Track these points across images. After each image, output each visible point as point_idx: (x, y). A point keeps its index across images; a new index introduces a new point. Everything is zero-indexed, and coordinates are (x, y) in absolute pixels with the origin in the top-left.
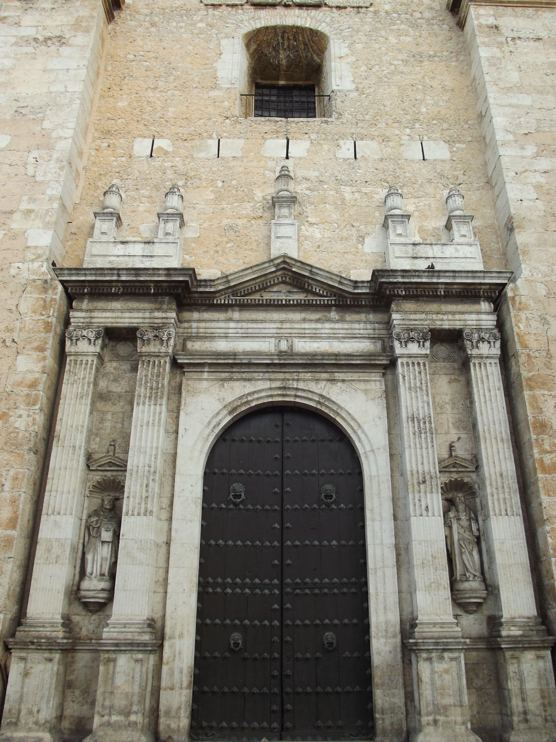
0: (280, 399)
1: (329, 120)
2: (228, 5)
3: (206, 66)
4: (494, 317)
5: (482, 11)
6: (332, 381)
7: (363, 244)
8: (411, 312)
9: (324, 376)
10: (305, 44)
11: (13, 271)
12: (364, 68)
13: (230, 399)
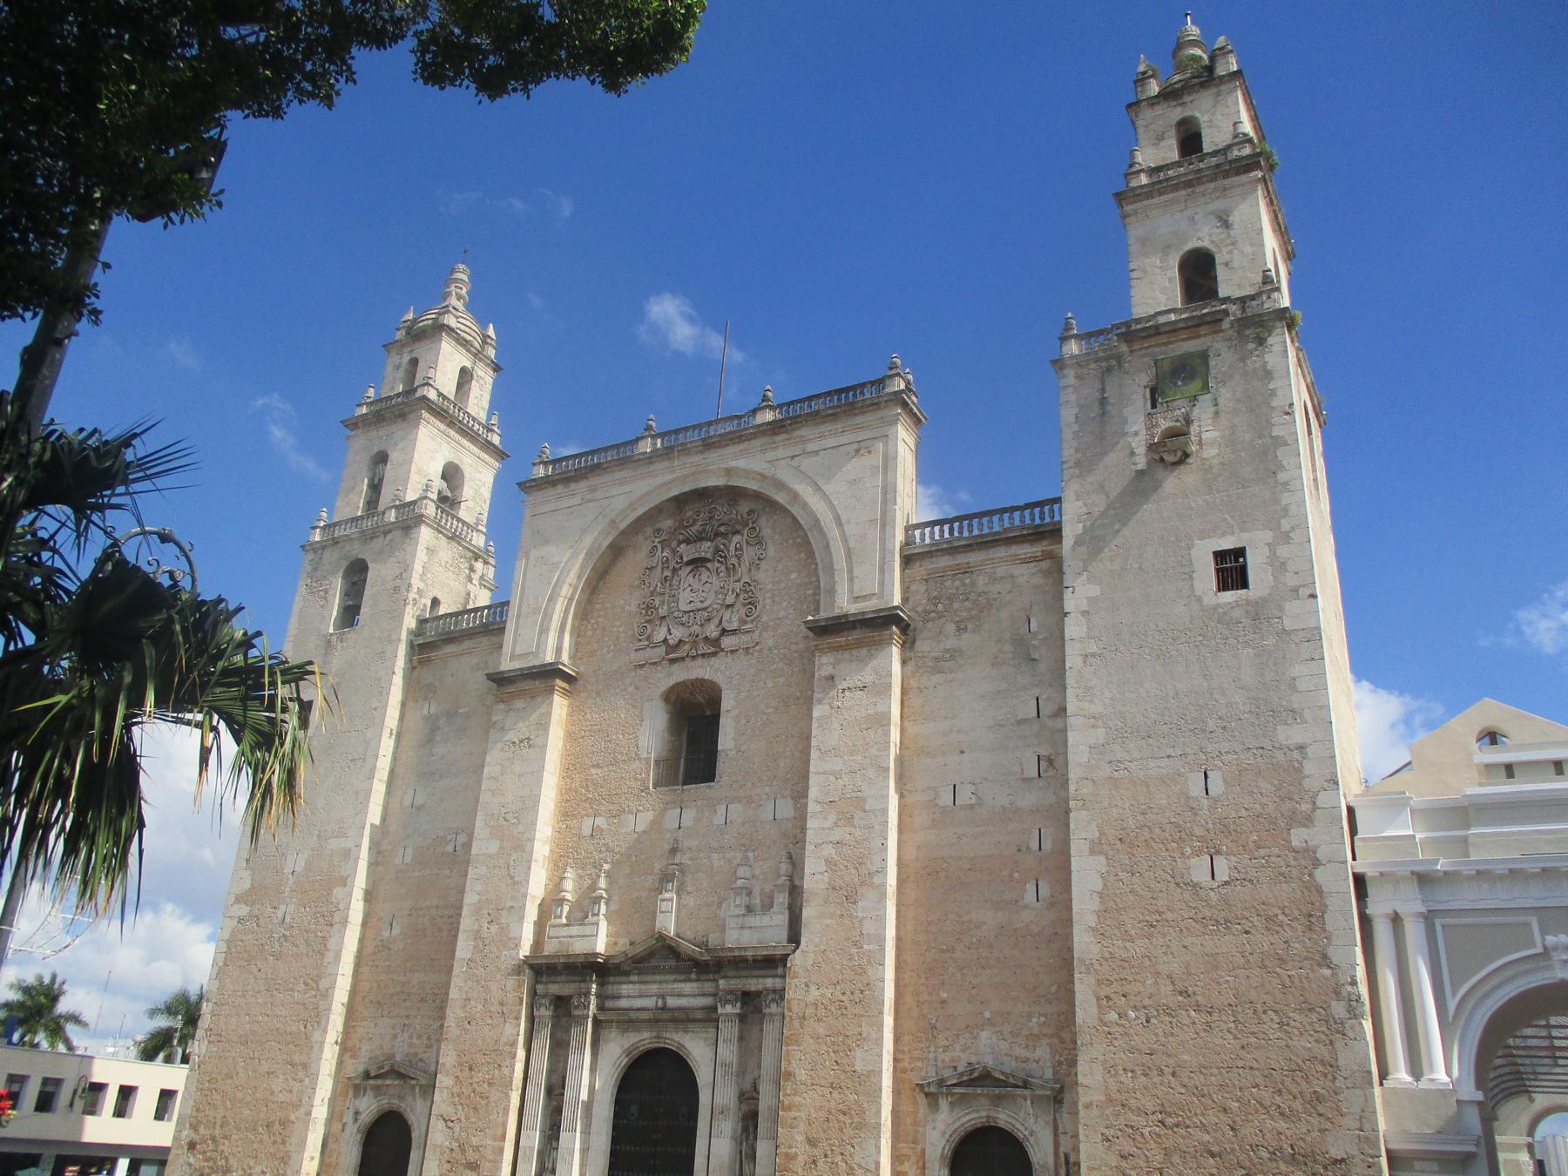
0: (656, 1045)
1: (712, 784)
2: (651, 664)
5: (824, 660)
6: (686, 1032)
8: (732, 978)
12: (744, 721)
13: (626, 1046)
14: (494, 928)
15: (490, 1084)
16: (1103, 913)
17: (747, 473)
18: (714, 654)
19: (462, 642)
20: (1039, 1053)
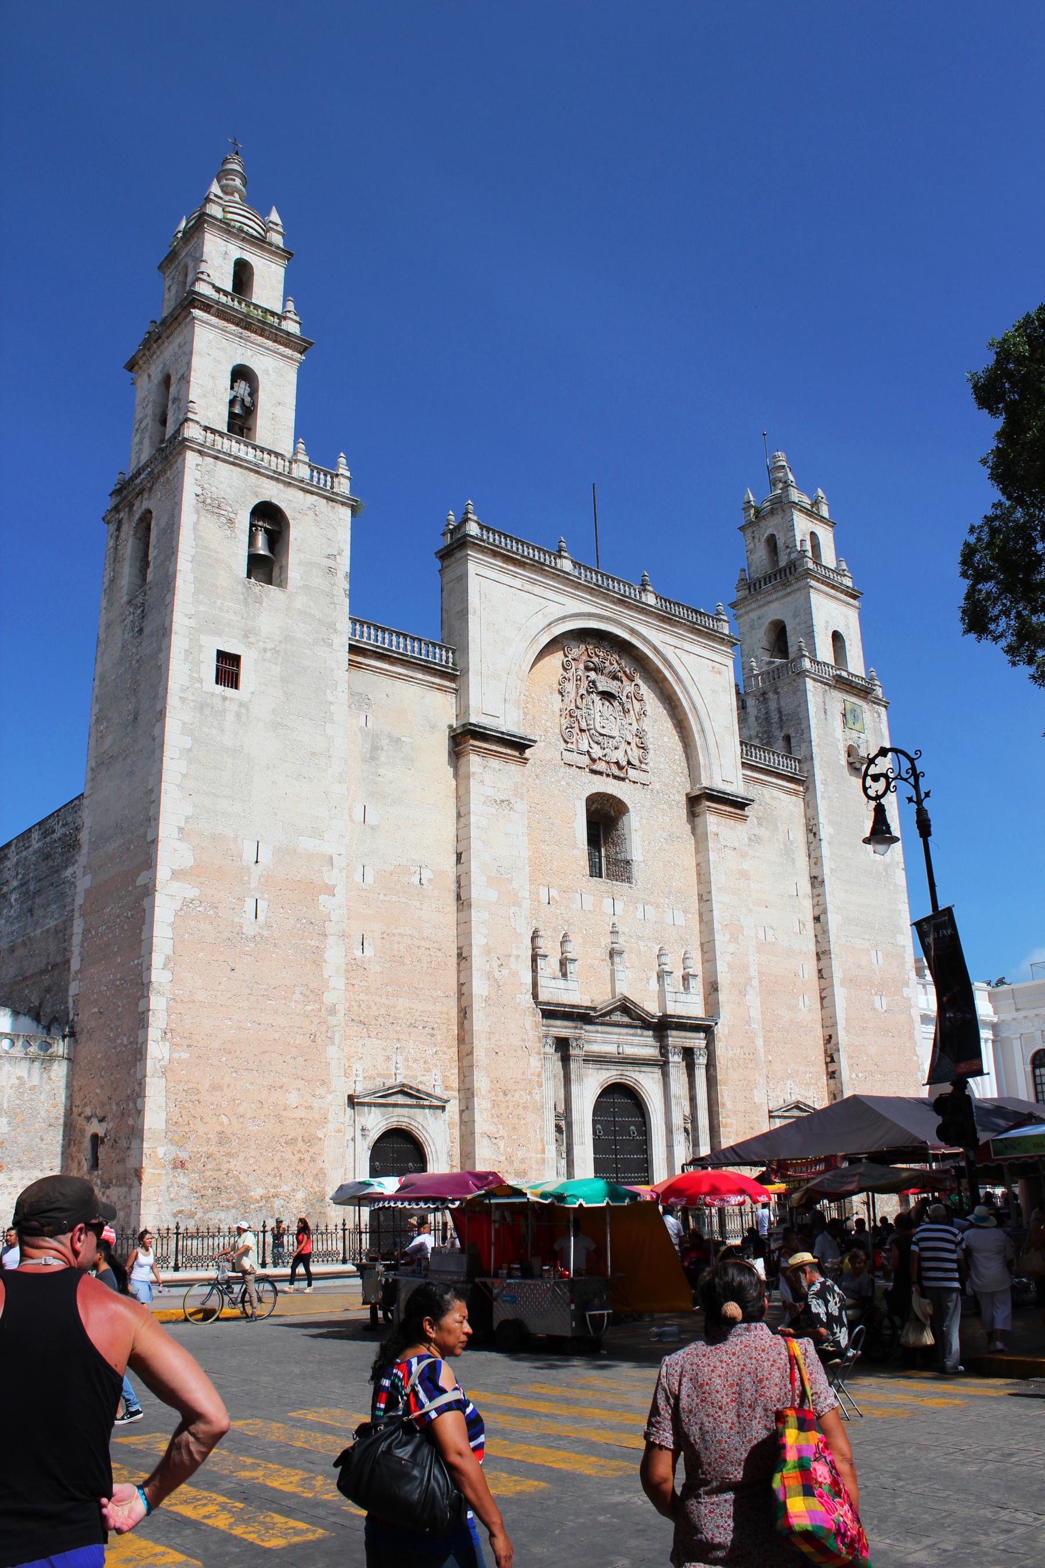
3: (569, 825)
4: (705, 1042)
7: (648, 983)
9: (637, 1069)
10: (611, 805)
11: (518, 1000)
14: (505, 972)
15: (525, 1108)
16: (847, 1019)
17: (645, 640)
18: (623, 779)
19: (392, 663)
20: (811, 1094)
